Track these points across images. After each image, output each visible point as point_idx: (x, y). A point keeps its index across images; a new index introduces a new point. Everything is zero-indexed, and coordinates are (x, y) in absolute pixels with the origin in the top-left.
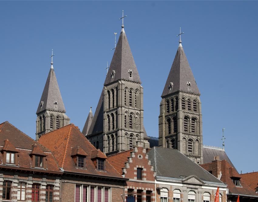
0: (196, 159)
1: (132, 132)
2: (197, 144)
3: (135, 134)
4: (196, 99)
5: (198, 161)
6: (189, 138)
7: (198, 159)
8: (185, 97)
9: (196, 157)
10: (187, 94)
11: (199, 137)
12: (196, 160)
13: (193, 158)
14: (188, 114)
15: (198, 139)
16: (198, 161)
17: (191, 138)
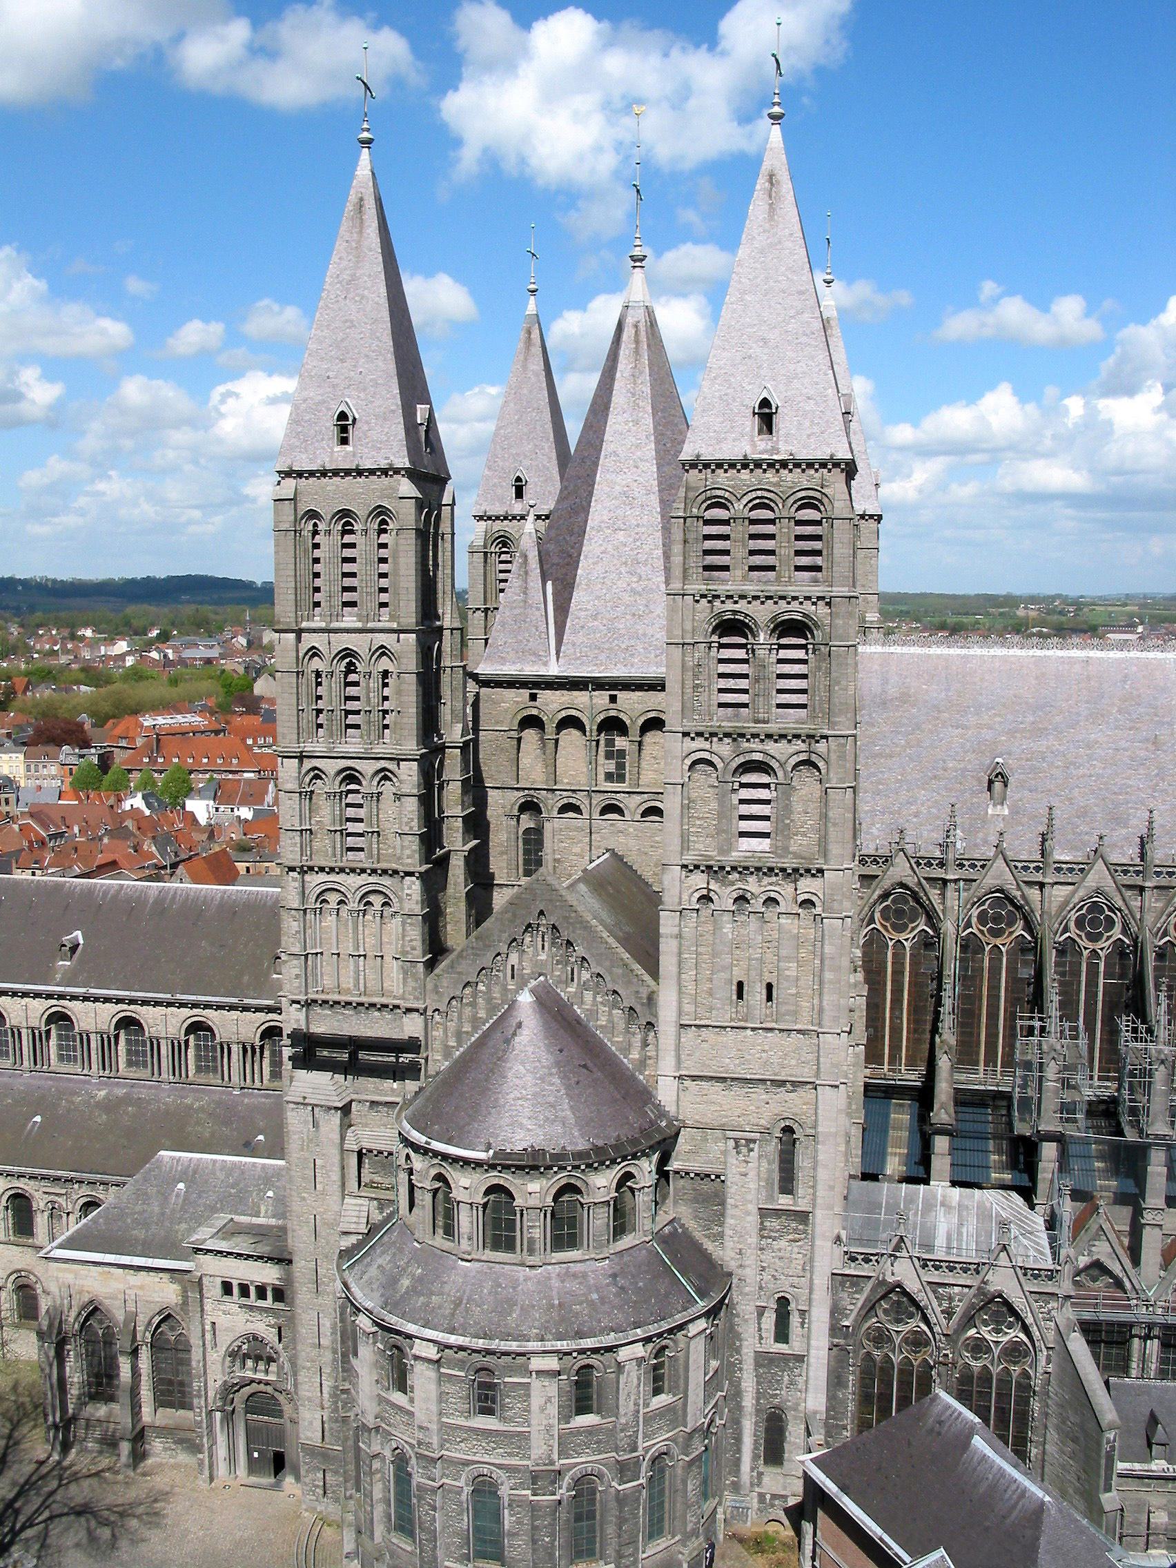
0: (796, 881)
1: (349, 763)
2: (806, 786)
3: (368, 768)
4: (817, 495)
5: (801, 898)
6: (741, 759)
7: (807, 885)
8: (727, 495)
9: (793, 875)
10: (745, 474)
11: (821, 747)
12: (789, 888)
13: (766, 880)
14: (742, 606)
15: (814, 758)
16: (806, 896)
17: (757, 757)
